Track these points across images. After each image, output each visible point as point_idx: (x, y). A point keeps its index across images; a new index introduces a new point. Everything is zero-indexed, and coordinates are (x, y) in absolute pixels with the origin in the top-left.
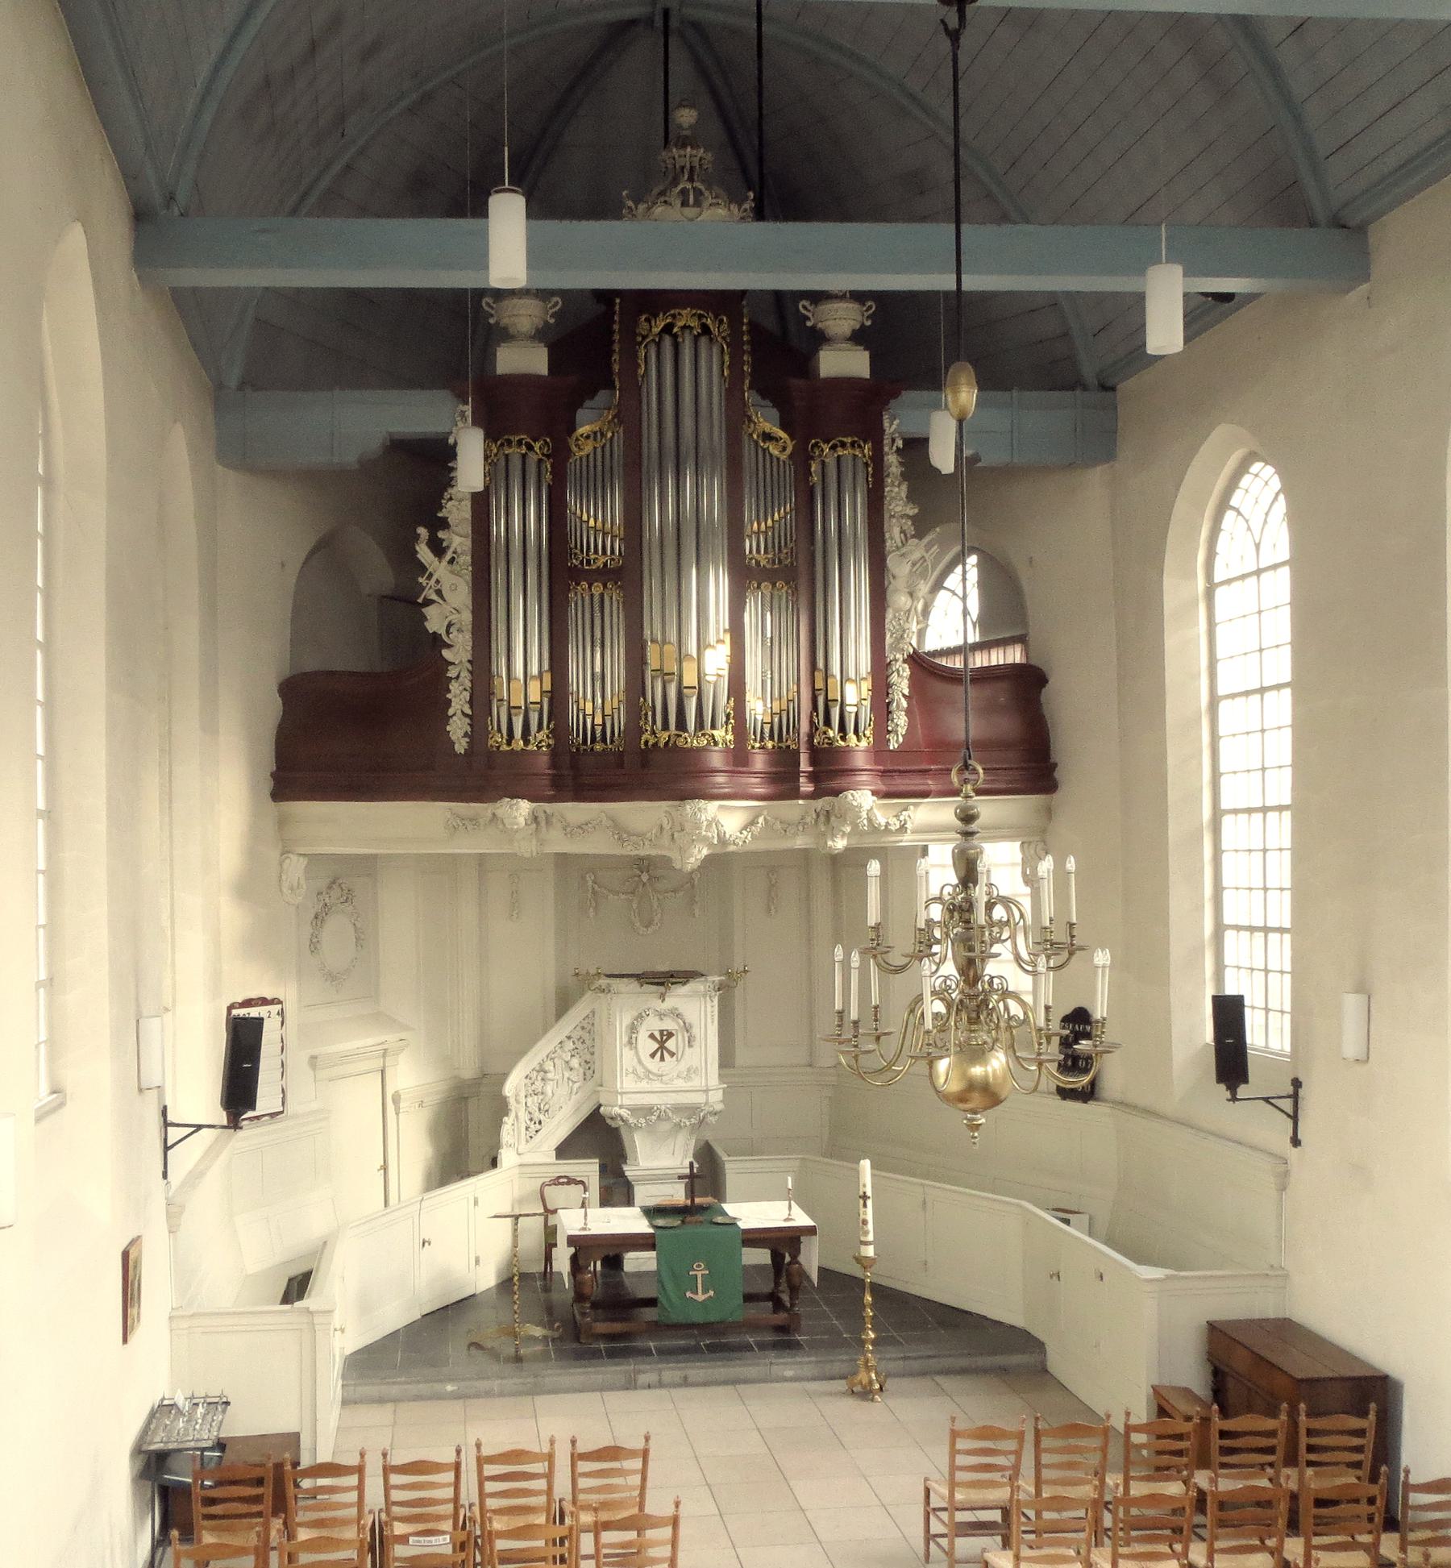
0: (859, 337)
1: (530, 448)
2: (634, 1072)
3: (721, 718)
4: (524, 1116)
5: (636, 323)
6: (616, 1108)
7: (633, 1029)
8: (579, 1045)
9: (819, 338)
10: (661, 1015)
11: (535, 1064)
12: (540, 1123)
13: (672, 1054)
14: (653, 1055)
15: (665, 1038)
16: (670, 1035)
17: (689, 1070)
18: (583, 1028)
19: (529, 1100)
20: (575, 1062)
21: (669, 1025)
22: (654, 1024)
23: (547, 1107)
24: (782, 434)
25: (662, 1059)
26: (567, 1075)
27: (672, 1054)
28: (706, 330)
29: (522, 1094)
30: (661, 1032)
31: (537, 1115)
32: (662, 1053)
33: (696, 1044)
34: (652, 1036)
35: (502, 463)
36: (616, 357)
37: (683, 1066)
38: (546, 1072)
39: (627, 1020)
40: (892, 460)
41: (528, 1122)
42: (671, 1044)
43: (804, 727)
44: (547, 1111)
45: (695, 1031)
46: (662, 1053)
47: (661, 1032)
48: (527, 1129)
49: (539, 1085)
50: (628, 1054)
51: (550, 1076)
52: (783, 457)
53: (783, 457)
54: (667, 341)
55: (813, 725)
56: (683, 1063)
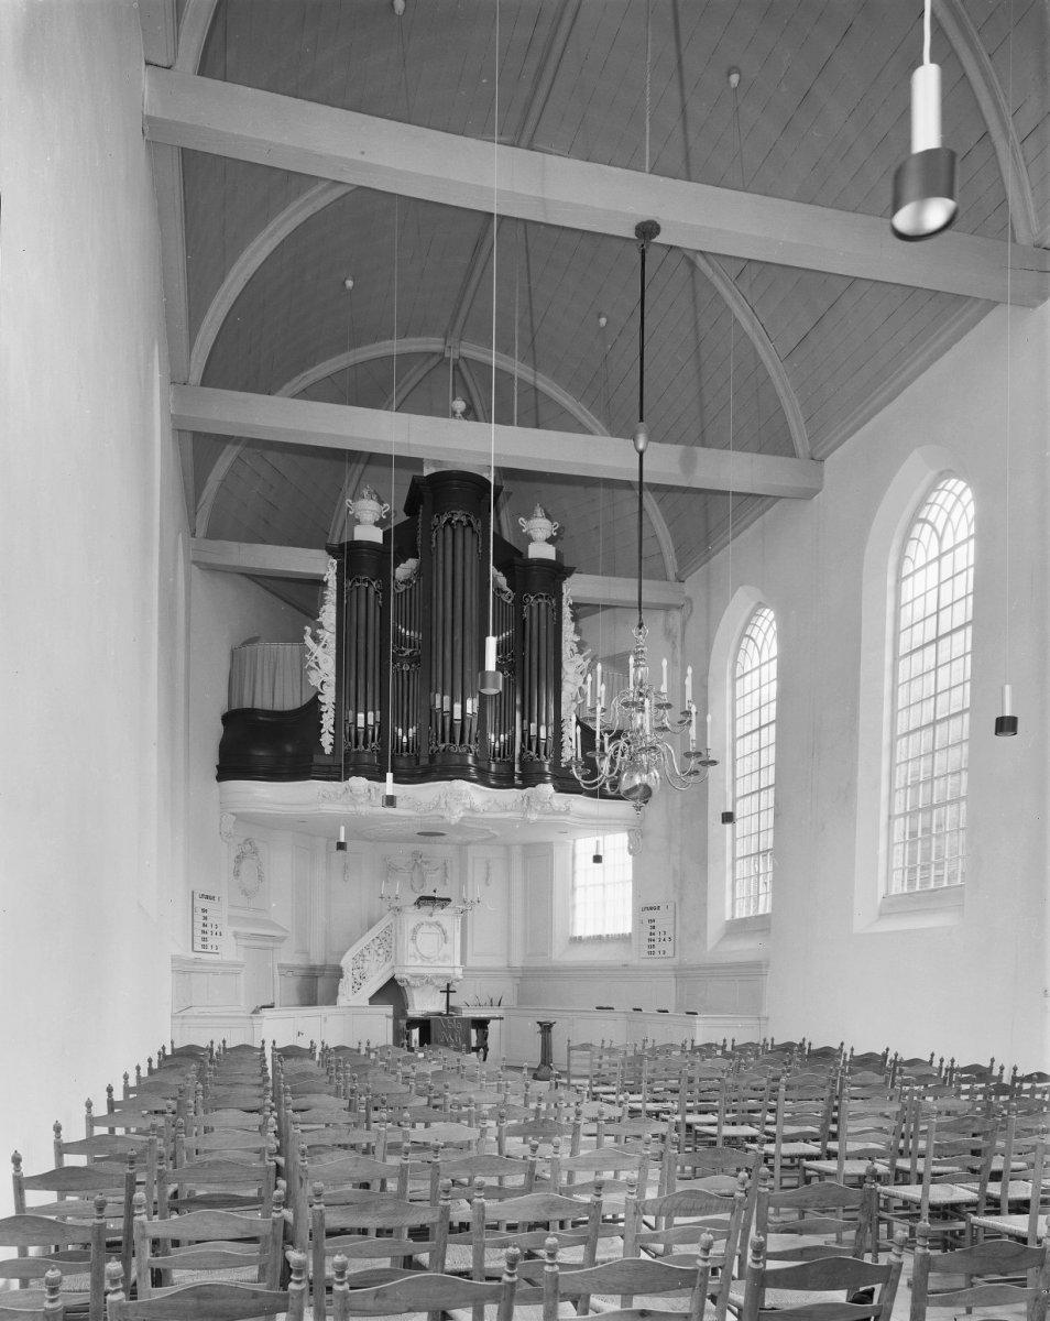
0: (550, 541)
1: (370, 583)
3: (473, 740)
5: (431, 519)
7: (415, 931)
9: (530, 539)
10: (430, 924)
19: (355, 972)
20: (381, 951)
24: (510, 591)
26: (376, 957)
28: (470, 524)
31: (359, 980)
35: (355, 593)
36: (419, 537)
39: (411, 927)
40: (567, 612)
43: (517, 751)
50: (411, 945)
52: (509, 602)
53: (509, 602)
54: (449, 529)
55: (522, 750)
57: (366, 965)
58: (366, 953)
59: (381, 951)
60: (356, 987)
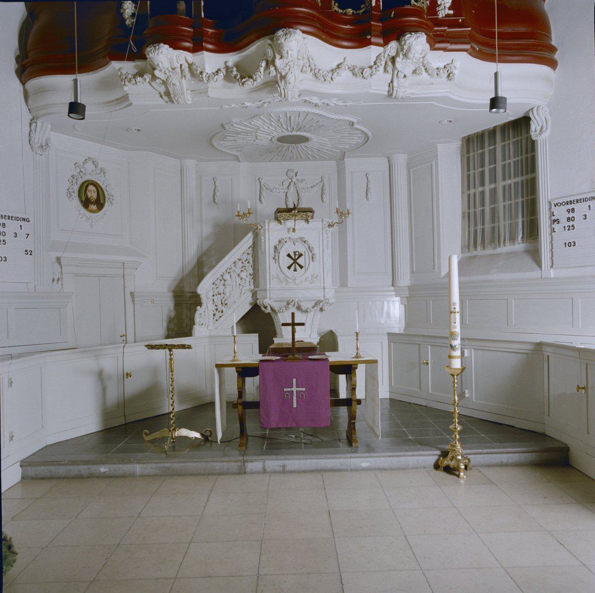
2: (278, 277)
4: (211, 307)
6: (270, 300)
8: (246, 263)
11: (219, 276)
12: (222, 312)
13: (301, 267)
14: (289, 268)
15: (297, 257)
16: (300, 255)
17: (312, 276)
18: (248, 254)
19: (215, 297)
21: (301, 248)
22: (289, 248)
23: (226, 302)
25: (295, 270)
27: (301, 267)
29: (211, 294)
30: (295, 253)
31: (220, 307)
32: (295, 266)
33: (317, 259)
34: (289, 255)
37: (308, 274)
38: (225, 280)
41: (215, 311)
42: (300, 261)
44: (226, 304)
45: (316, 251)
46: (295, 266)
47: (295, 253)
48: (214, 315)
49: (221, 288)
51: (227, 283)
56: (308, 272)
57: (227, 291)
58: (227, 277)
59: (243, 275)
60: (218, 314)
